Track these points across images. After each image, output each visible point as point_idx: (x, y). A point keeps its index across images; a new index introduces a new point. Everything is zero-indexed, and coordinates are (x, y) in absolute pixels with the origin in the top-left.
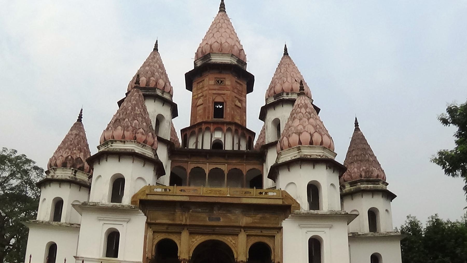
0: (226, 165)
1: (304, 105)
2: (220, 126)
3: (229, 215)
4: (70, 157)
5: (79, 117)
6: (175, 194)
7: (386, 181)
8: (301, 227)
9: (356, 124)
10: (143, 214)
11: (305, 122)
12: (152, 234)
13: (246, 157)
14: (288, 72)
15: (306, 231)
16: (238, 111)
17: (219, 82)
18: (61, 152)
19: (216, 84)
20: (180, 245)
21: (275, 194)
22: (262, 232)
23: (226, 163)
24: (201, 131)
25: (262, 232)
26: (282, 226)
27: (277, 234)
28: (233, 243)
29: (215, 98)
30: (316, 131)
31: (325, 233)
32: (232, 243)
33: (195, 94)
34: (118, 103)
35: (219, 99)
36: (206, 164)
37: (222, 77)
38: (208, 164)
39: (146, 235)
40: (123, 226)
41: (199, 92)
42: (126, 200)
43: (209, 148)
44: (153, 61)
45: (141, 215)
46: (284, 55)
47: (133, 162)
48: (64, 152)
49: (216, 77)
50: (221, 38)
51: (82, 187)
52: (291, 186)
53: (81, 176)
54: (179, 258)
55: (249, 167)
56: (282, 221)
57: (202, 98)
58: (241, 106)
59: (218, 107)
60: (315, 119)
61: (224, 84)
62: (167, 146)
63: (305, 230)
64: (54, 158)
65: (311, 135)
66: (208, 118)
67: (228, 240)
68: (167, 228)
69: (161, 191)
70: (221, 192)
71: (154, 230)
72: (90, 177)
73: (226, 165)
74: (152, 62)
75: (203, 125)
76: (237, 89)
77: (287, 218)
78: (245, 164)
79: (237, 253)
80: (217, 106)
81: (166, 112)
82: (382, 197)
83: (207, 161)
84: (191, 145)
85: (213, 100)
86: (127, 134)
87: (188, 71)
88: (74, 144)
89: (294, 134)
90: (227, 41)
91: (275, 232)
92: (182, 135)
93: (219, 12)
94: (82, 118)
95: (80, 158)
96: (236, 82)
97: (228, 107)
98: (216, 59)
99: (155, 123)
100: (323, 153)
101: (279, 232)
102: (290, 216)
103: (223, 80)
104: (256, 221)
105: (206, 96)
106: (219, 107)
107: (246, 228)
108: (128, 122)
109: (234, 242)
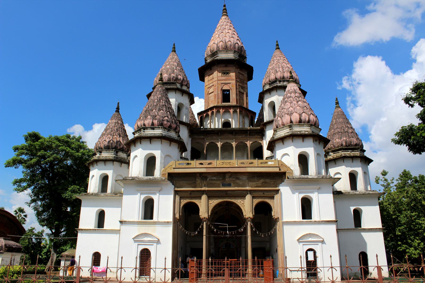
1: (293, 91)
3: (238, 181)
4: (111, 141)
6: (195, 167)
7: (364, 149)
10: (171, 184)
11: (295, 105)
13: (250, 133)
14: (280, 64)
16: (241, 96)
17: (226, 73)
18: (104, 138)
19: (224, 76)
20: (201, 206)
21: (273, 163)
22: (264, 193)
23: (234, 138)
25: (264, 193)
28: (242, 204)
29: (223, 87)
30: (304, 112)
32: (241, 203)
34: (147, 96)
35: (226, 88)
37: (227, 70)
42: (157, 173)
43: (220, 127)
44: (172, 60)
48: (107, 138)
50: (225, 38)
51: (123, 164)
52: (286, 157)
53: (122, 155)
54: (200, 217)
57: (212, 87)
59: (225, 93)
60: (302, 102)
62: (188, 127)
64: (99, 142)
65: (300, 115)
66: (218, 102)
67: (238, 202)
68: (190, 194)
70: (230, 163)
72: (129, 155)
74: (172, 62)
78: (248, 138)
81: (185, 100)
82: (361, 162)
83: (219, 137)
85: (221, 89)
86: (156, 122)
87: (200, 67)
88: (114, 130)
89: (286, 115)
91: (274, 194)
94: (119, 109)
95: (120, 141)
96: (239, 72)
98: (222, 56)
99: (177, 110)
100: (310, 129)
104: (259, 185)
106: (226, 93)
107: (251, 192)
108: (156, 112)
109: (243, 203)
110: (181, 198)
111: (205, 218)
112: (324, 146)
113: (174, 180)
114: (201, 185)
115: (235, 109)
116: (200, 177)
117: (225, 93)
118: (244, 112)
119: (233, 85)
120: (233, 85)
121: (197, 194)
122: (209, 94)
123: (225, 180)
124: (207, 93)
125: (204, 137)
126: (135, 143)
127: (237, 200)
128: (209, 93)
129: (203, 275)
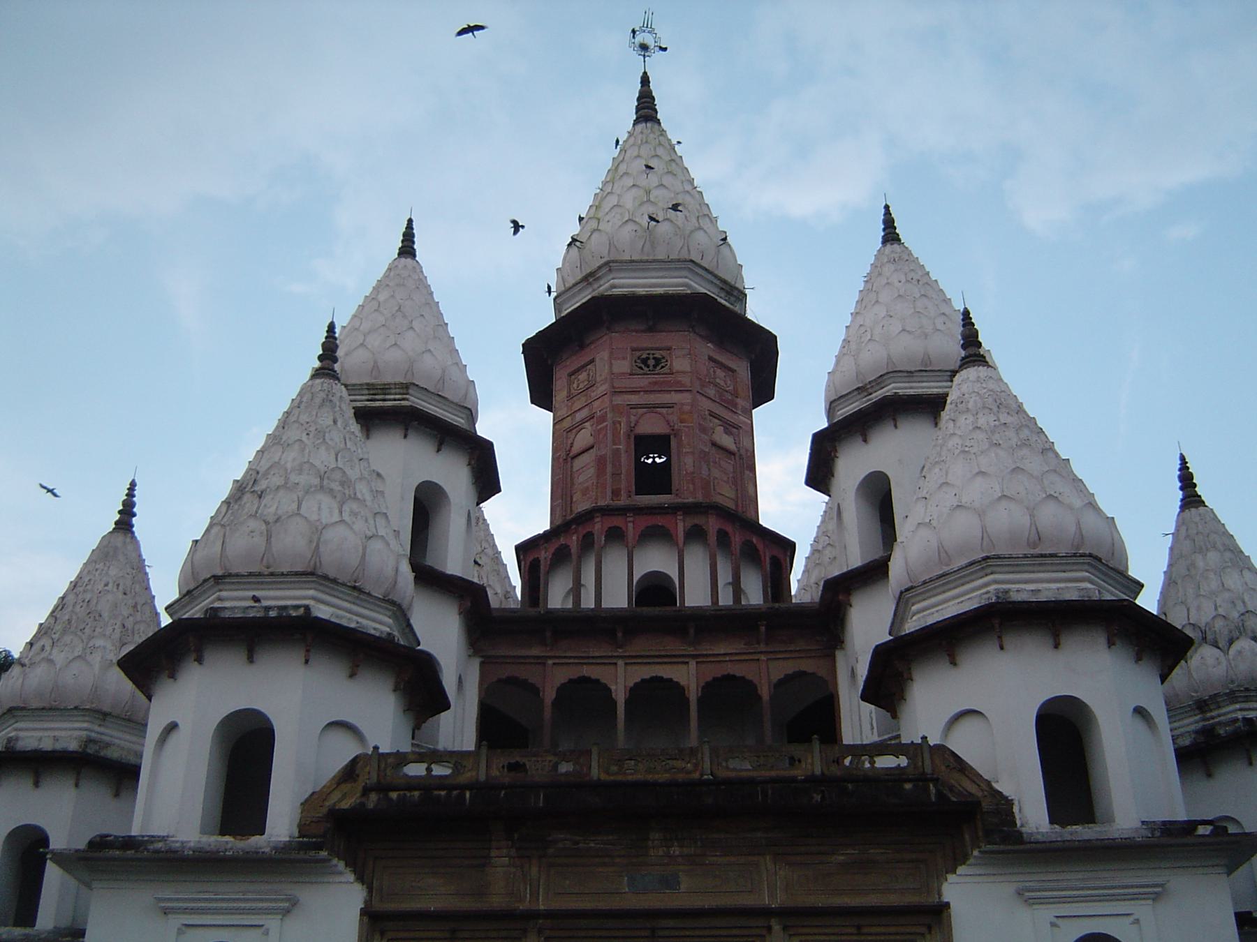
0: (693, 664)
2: (660, 520)
5: (120, 512)
8: (1027, 898)
9: (1187, 480)
10: (351, 877)
17: (649, 363)
22: (859, 927)
24: (592, 544)
25: (859, 927)
26: (946, 899)
27: (928, 936)
29: (637, 422)
31: (1137, 921)
33: (563, 412)
35: (651, 426)
36: (616, 664)
38: (620, 663)
40: (267, 933)
41: (577, 406)
45: (343, 879)
47: (307, 662)
49: (634, 345)
52: (967, 725)
55: (780, 669)
56: (941, 878)
58: (733, 447)
59: (650, 461)
61: (665, 370)
62: (461, 598)
63: (1046, 913)
66: (616, 493)
69: (424, 773)
73: (693, 664)
77: (964, 863)
78: (763, 657)
80: (648, 458)
84: (557, 597)
85: (631, 430)
90: (664, 183)
91: (913, 929)
92: (523, 563)
93: (636, 122)
94: (134, 515)
96: (711, 359)
102: (976, 853)
103: (664, 358)
105: (603, 419)
106: (654, 461)
115: (692, 521)
117: (650, 461)
118: (737, 539)
122: (573, 458)
124: (564, 455)
128: (571, 454)
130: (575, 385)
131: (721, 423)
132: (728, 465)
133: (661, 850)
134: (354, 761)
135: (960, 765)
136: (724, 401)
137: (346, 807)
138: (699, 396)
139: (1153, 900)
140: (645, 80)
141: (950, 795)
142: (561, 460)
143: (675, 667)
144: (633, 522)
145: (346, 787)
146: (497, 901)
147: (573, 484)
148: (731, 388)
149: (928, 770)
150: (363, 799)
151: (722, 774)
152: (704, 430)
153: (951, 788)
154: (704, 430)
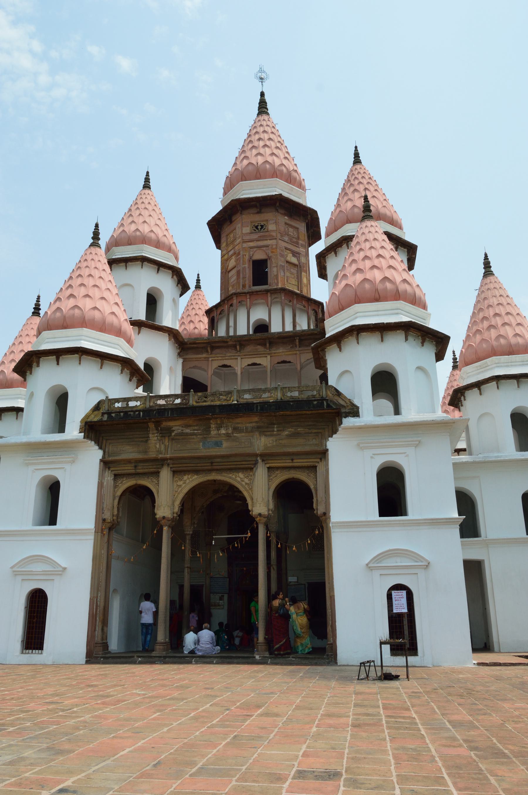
0: (269, 357)
5: (34, 308)
9: (487, 265)
10: (97, 447)
12: (112, 478)
13: (301, 341)
15: (372, 455)
16: (292, 270)
17: (259, 228)
19: (254, 231)
20: (158, 493)
22: (292, 460)
23: (269, 354)
25: (292, 460)
27: (320, 463)
28: (246, 484)
31: (407, 456)
32: (244, 483)
33: (224, 252)
35: (259, 256)
38: (239, 358)
39: (101, 481)
40: (65, 471)
46: (354, 164)
52: (346, 377)
56: (327, 440)
57: (233, 257)
61: (266, 230)
63: (369, 453)
66: (244, 286)
68: (135, 466)
69: (125, 406)
71: (116, 472)
75: (235, 298)
76: (288, 235)
77: (336, 433)
78: (298, 352)
79: (252, 499)
83: (239, 354)
84: (222, 332)
87: (210, 218)
93: (258, 115)
96: (286, 224)
97: (274, 267)
101: (323, 459)
103: (265, 225)
107: (265, 457)
110: (116, 476)
111: (164, 518)
112: (436, 350)
113: (102, 440)
114: (158, 446)
116: (157, 429)
119: (274, 249)
120: (274, 249)
121: (151, 467)
123: (210, 434)
125: (208, 356)
126: (32, 369)
127: (234, 476)
129: (158, 647)
130: (229, 240)
131: (291, 252)
132: (294, 271)
133: (215, 432)
134: (99, 403)
135: (338, 393)
136: (293, 242)
137: (96, 420)
138: (280, 241)
139: (415, 447)
140: (262, 94)
141: (333, 406)
142: (224, 273)
143: (261, 358)
144: (249, 298)
145: (96, 412)
146: (152, 455)
147: (228, 283)
148: (297, 236)
149: (324, 396)
150: (102, 417)
151: (242, 401)
152: (282, 256)
153: (334, 403)
154: (282, 256)
